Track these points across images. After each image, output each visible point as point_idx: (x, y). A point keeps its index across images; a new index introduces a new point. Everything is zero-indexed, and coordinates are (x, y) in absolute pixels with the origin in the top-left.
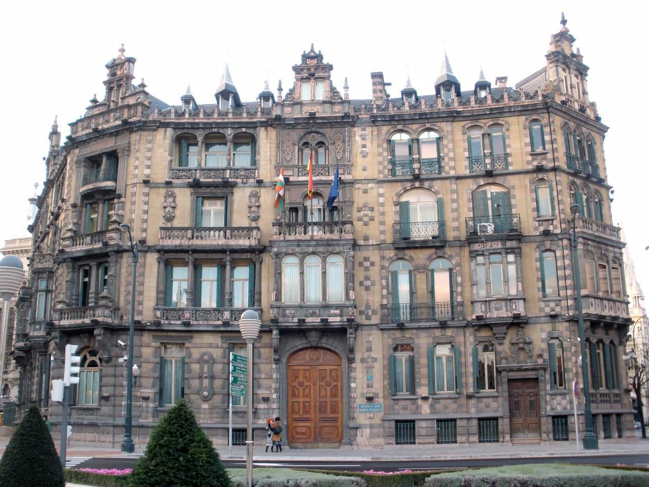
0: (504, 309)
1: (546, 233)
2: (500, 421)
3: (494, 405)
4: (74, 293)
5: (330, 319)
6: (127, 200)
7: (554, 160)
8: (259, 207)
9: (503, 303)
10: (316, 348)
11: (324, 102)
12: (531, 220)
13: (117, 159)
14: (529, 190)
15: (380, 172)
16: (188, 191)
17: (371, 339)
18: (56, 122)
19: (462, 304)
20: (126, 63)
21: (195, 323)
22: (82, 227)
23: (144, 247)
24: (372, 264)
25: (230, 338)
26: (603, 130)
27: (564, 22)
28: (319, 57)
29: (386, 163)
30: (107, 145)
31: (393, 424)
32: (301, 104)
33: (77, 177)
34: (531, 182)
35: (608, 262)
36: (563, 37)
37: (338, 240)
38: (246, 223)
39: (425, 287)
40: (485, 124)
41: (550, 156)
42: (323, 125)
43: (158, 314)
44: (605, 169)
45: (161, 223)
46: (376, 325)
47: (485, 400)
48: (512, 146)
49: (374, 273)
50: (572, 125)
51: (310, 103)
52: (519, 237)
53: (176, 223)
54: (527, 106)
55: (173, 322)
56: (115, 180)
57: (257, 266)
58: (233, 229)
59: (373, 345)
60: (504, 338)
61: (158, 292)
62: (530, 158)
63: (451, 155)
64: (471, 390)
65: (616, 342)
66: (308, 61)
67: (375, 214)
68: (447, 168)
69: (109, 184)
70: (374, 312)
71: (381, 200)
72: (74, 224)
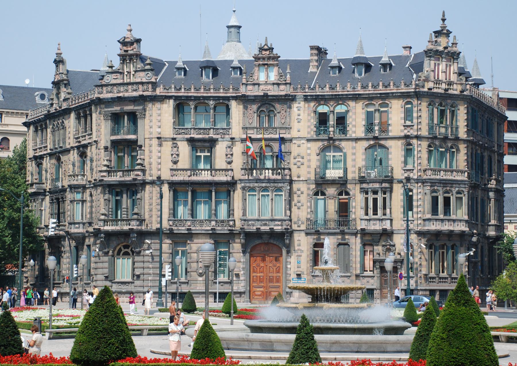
0: (378, 225)
1: (408, 179)
2: (375, 292)
5: (275, 228)
6: (146, 149)
8: (232, 155)
9: (378, 222)
10: (267, 244)
11: (274, 84)
12: (400, 168)
14: (400, 150)
15: (308, 133)
17: (300, 238)
19: (355, 220)
21: (194, 228)
23: (159, 181)
24: (302, 193)
27: (444, 20)
28: (271, 49)
29: (313, 127)
32: (259, 85)
33: (106, 126)
35: (452, 195)
37: (280, 180)
38: (224, 166)
39: (333, 207)
41: (415, 127)
42: (273, 100)
43: (171, 223)
45: (171, 165)
46: (303, 231)
47: (366, 279)
48: (393, 119)
49: (304, 198)
51: (264, 84)
52: (390, 181)
53: (180, 166)
54: (404, 93)
55: (180, 228)
57: (232, 193)
58: (216, 170)
59: (302, 243)
61: (170, 209)
62: (403, 128)
63: (354, 123)
64: (358, 272)
66: (264, 52)
67: (305, 161)
68: (350, 132)
69: (132, 137)
70: (303, 223)
71: (309, 151)
72: (107, 160)
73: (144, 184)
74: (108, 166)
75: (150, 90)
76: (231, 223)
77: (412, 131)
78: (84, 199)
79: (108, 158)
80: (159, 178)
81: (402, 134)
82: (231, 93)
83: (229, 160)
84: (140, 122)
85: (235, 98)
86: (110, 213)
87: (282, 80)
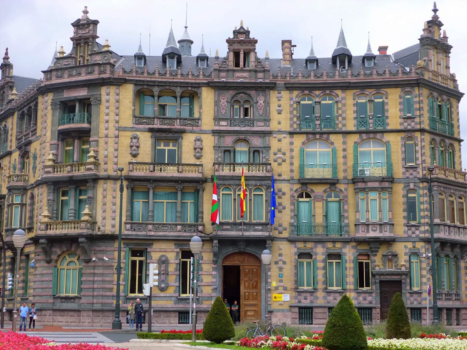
0: (378, 231)
2: (374, 311)
3: (369, 298)
4: (55, 208)
7: (420, 123)
13: (89, 105)
15: (291, 126)
16: (148, 135)
18: (7, 54)
20: (91, 25)
22: (59, 157)
24: (284, 194)
25: (181, 245)
26: (459, 96)
27: (435, 10)
28: (247, 33)
29: (295, 119)
30: (82, 93)
31: (297, 310)
33: (53, 115)
34: (402, 138)
36: (434, 23)
38: (193, 161)
40: (370, 93)
41: (417, 120)
44: (459, 126)
45: (129, 158)
50: (435, 94)
52: (391, 180)
53: (139, 159)
56: (89, 123)
57: (201, 193)
60: (378, 251)
62: (402, 121)
63: (344, 115)
65: (459, 257)
67: (287, 157)
69: (86, 125)
70: (285, 229)
72: (53, 154)
73: (96, 179)
74: (54, 161)
75: (108, 72)
76: (200, 228)
77: (413, 124)
78: (24, 203)
79: (54, 152)
81: (401, 128)
82: (202, 79)
83: (198, 155)
84: (94, 109)
86: (55, 215)
87: (259, 67)
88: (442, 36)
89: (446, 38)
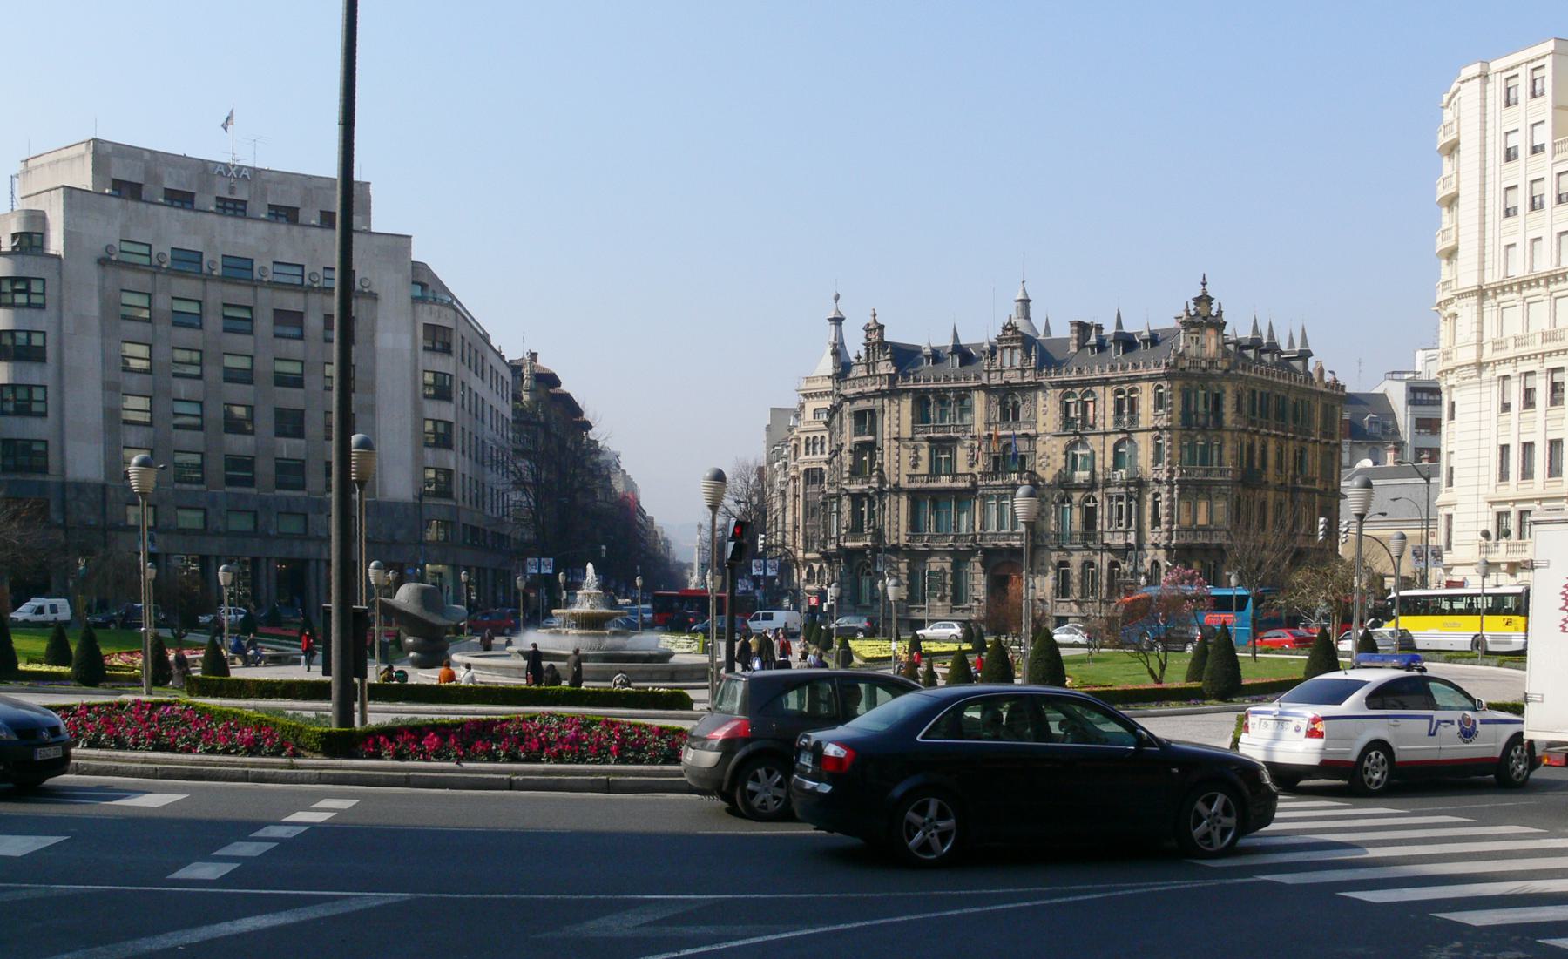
23: (897, 490)
27: (1204, 284)
53: (918, 472)
69: (870, 438)
80: (896, 485)
85: (977, 388)
88: (1214, 313)
89: (1220, 312)
